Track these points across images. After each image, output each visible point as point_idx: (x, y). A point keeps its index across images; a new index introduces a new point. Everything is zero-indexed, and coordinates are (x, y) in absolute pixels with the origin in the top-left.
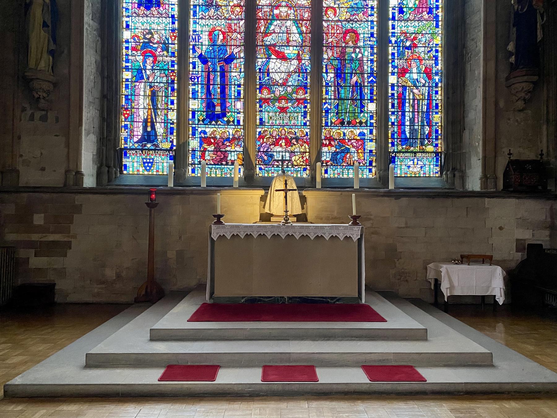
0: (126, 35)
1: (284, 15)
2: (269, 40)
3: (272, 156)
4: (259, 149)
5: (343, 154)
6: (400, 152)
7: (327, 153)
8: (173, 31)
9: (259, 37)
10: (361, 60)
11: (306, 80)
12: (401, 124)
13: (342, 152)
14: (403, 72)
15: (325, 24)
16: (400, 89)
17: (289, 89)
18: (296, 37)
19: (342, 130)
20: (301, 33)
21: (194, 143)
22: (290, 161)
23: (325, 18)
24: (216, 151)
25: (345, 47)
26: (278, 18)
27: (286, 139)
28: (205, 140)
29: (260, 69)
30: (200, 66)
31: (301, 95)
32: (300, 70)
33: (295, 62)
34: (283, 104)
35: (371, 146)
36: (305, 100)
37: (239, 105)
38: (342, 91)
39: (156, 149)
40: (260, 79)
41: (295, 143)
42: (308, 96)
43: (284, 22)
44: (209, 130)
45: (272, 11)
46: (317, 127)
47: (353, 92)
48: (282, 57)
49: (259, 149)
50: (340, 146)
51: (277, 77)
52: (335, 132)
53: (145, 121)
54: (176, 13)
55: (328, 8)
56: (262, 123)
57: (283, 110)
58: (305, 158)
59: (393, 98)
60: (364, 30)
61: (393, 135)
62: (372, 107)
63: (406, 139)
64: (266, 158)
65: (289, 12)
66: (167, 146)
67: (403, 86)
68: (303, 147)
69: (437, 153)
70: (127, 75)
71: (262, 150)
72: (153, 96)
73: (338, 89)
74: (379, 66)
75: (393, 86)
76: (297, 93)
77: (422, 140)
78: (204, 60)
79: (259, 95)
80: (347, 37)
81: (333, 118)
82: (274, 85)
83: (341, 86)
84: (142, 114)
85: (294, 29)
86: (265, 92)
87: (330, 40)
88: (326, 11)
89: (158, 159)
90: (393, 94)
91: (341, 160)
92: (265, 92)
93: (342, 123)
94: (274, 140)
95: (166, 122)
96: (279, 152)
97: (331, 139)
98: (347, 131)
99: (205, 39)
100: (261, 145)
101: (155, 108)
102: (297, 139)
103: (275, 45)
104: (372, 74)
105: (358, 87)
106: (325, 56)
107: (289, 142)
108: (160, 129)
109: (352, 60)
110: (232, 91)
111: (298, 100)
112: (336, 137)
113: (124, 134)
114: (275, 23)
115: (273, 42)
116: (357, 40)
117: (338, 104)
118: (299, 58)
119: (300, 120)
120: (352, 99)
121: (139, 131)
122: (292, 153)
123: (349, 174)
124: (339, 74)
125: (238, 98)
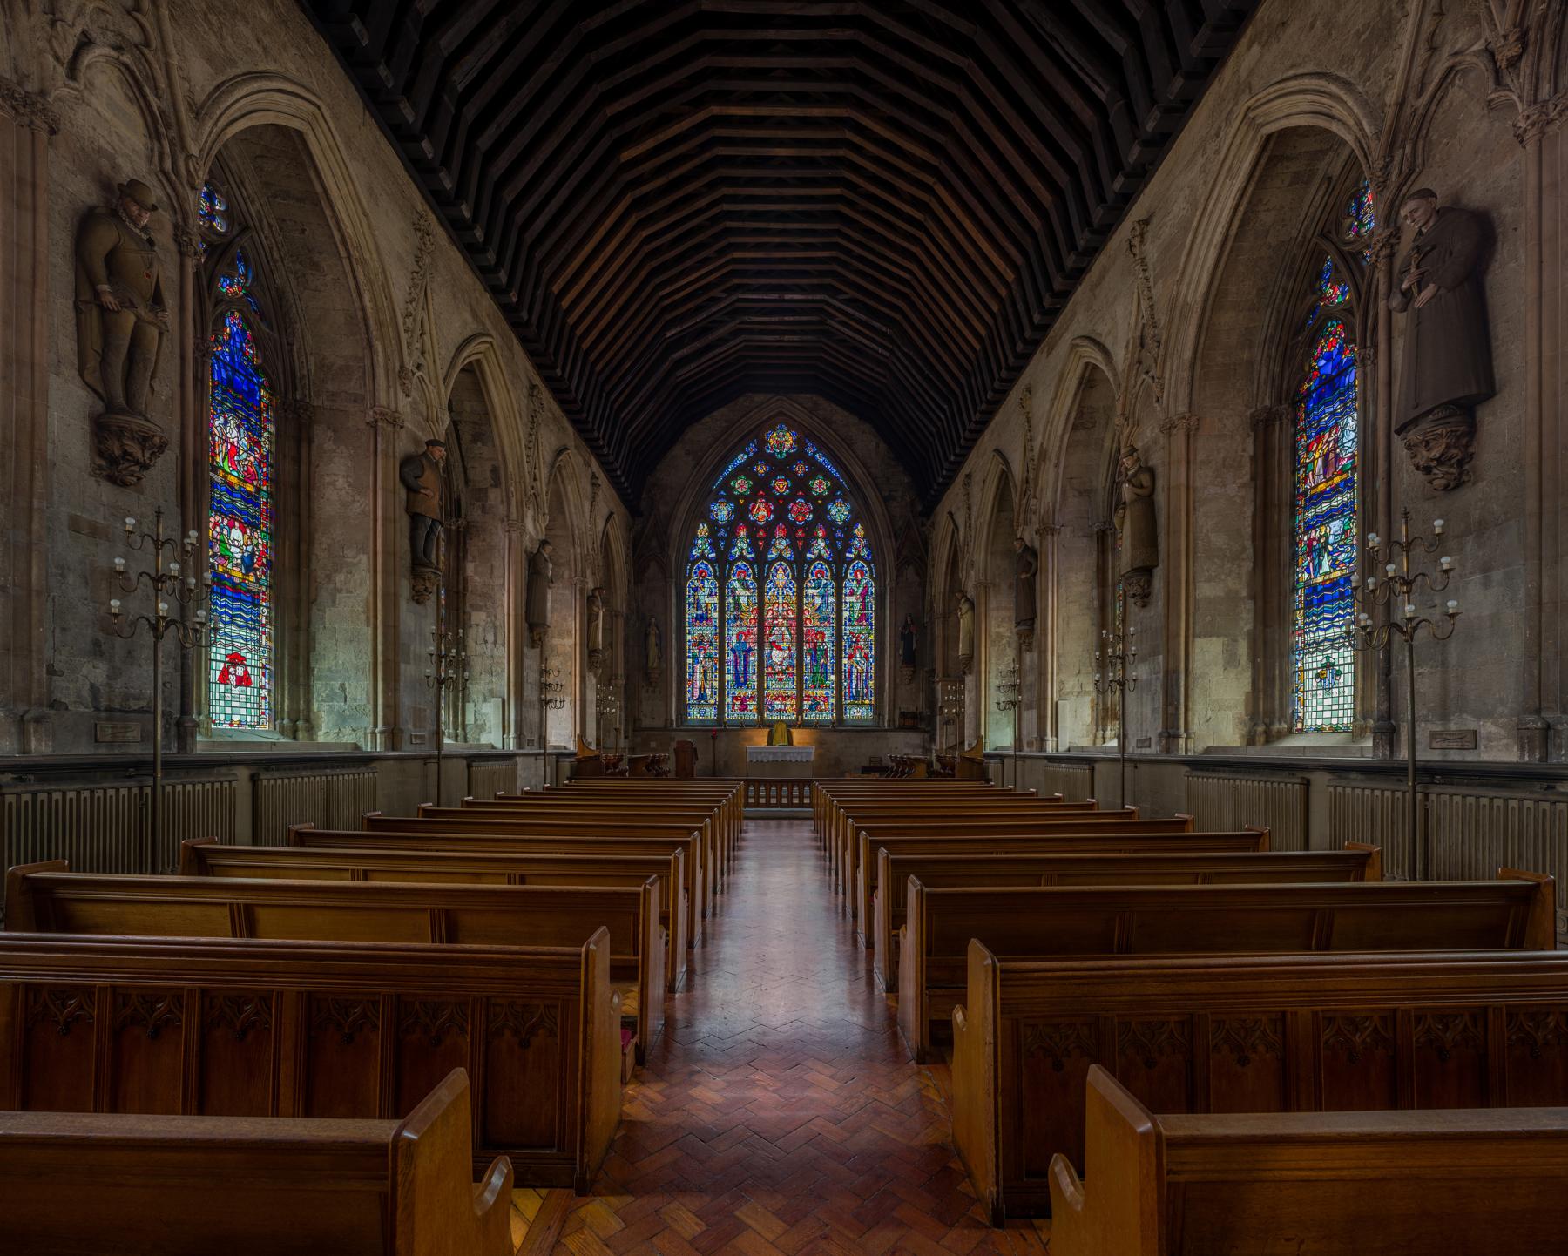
0: (689, 637)
2: (771, 638)
8: (716, 634)
10: (826, 650)
12: (850, 687)
14: (850, 657)
18: (787, 637)
19: (816, 691)
20: (790, 634)
21: (728, 700)
24: (741, 705)
26: (777, 625)
28: (735, 698)
30: (731, 656)
31: (791, 671)
32: (790, 656)
33: (787, 652)
34: (780, 676)
35: (832, 700)
37: (754, 677)
39: (707, 704)
42: (795, 671)
44: (737, 692)
46: (800, 689)
48: (780, 649)
51: (776, 660)
52: (810, 692)
53: (700, 688)
54: (717, 624)
56: (768, 688)
57: (780, 680)
60: (828, 633)
62: (833, 677)
66: (712, 701)
69: (871, 705)
70: (689, 661)
72: (705, 673)
74: (837, 653)
78: (734, 652)
81: (809, 684)
84: (698, 684)
89: (708, 710)
93: (815, 687)
95: (712, 688)
96: (778, 704)
97: (808, 696)
98: (818, 692)
99: (734, 639)
101: (706, 680)
104: (832, 658)
105: (825, 665)
107: (784, 699)
108: (709, 692)
110: (751, 669)
113: (688, 695)
116: (824, 638)
118: (789, 649)
119: (791, 686)
121: (697, 693)
122: (786, 705)
123: (821, 717)
124: (814, 658)
125: (754, 673)
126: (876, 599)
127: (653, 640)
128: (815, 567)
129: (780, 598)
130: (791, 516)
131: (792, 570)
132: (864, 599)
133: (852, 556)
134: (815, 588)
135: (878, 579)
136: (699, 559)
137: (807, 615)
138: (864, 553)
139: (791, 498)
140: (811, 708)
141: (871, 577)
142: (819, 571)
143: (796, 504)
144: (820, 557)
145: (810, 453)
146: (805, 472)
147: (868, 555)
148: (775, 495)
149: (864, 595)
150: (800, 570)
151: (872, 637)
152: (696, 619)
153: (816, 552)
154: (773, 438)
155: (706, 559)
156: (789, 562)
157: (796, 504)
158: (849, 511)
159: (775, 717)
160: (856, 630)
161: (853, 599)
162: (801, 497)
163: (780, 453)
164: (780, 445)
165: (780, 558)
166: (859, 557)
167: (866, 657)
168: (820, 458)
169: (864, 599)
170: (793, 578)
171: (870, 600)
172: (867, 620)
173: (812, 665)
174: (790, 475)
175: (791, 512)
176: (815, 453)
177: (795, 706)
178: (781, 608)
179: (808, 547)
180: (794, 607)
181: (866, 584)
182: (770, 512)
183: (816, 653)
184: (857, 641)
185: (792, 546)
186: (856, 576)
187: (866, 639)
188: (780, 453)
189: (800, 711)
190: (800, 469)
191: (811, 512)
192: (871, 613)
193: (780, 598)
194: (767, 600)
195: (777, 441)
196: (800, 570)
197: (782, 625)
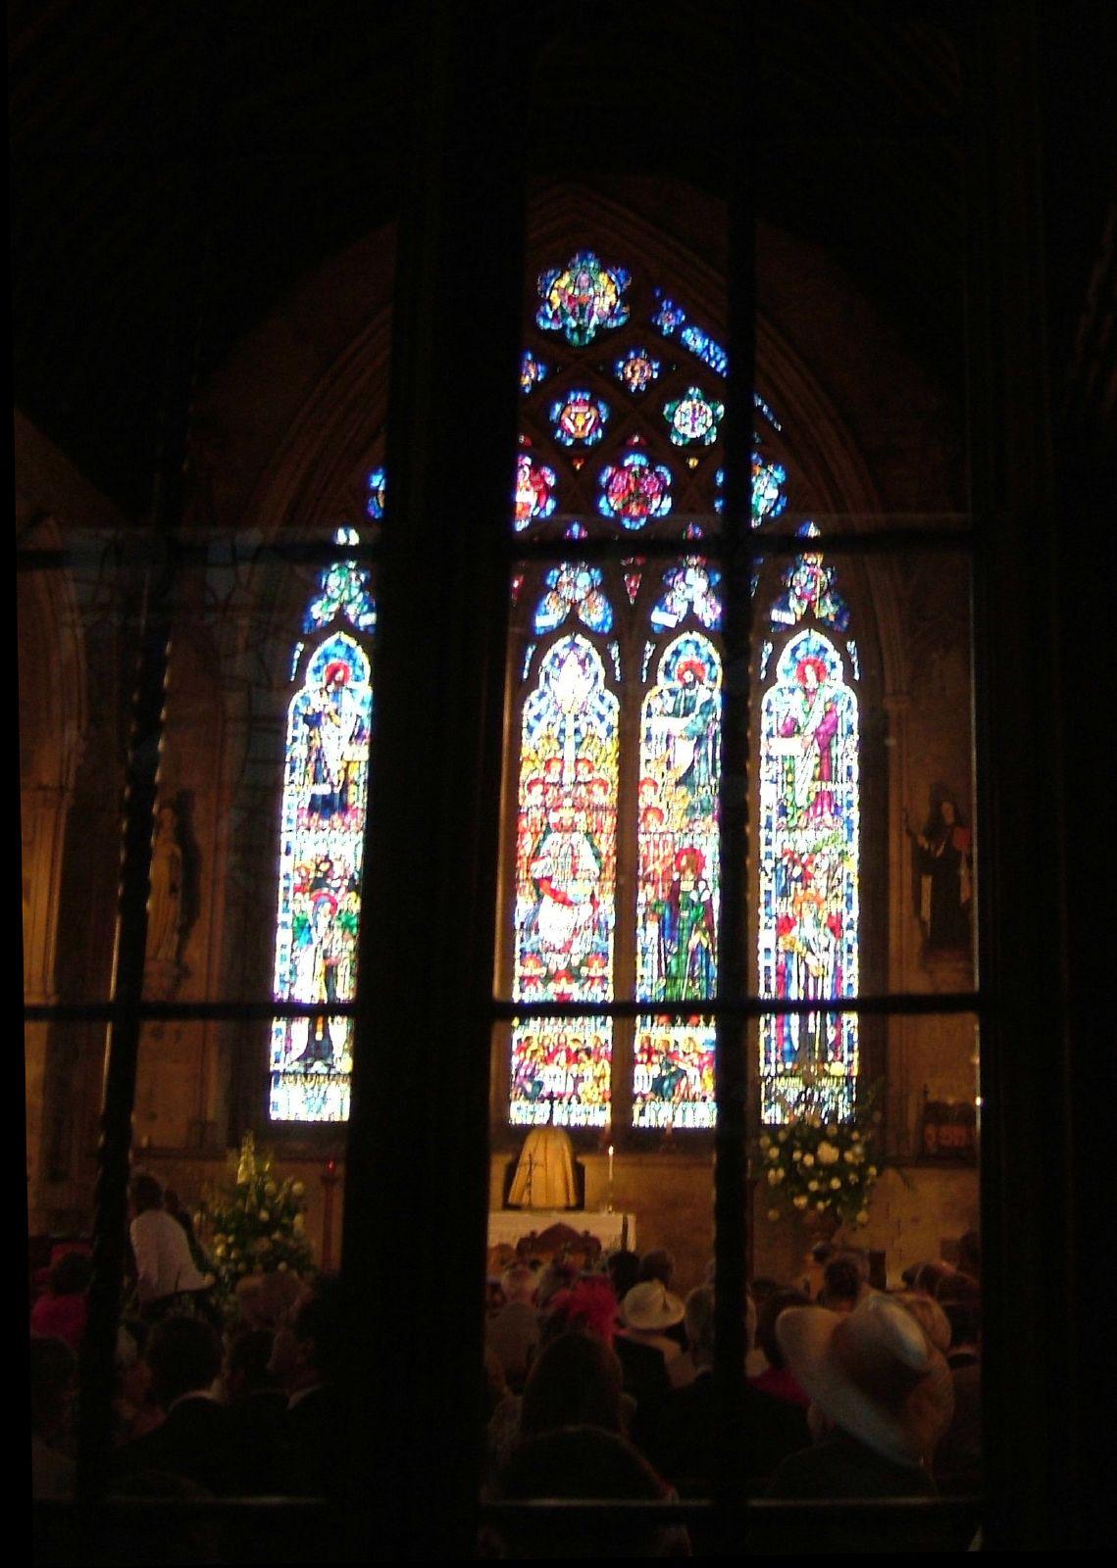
1: (567, 823)
2: (539, 869)
3: (540, 1084)
4: (517, 1071)
5: (673, 1081)
6: (779, 1075)
7: (644, 1076)
9: (522, 863)
11: (607, 940)
13: (673, 1075)
14: (785, 925)
15: (642, 839)
16: (782, 958)
17: (575, 962)
18: (588, 862)
20: (598, 856)
22: (575, 1093)
23: (642, 828)
25: (679, 881)
26: (560, 828)
27: (568, 1050)
29: (522, 924)
31: (596, 970)
32: (597, 926)
33: (586, 910)
36: (604, 978)
38: (673, 962)
40: (522, 941)
41: (585, 1058)
42: (609, 971)
43: (567, 836)
45: (546, 814)
47: (693, 964)
49: (517, 1071)
50: (669, 1066)
55: (648, 808)
58: (602, 1089)
59: (768, 976)
61: (768, 1040)
63: (792, 1050)
64: (529, 1087)
65: (576, 819)
67: (786, 952)
68: (600, 1066)
71: (522, 1073)
73: (666, 959)
75: (767, 950)
76: (589, 965)
77: (824, 1053)
79: (519, 970)
80: (684, 862)
82: (547, 951)
83: (668, 952)
85: (585, 850)
86: (531, 963)
87: (650, 869)
88: (645, 815)
90: (767, 968)
91: (670, 1092)
92: (531, 963)
94: (546, 1054)
97: (650, 1051)
100: (520, 1065)
102: (588, 1052)
103: (549, 879)
106: (641, 898)
109: (692, 905)
111: (588, 978)
112: (658, 1045)
114: (551, 838)
115: (546, 874)
117: (665, 988)
120: (692, 976)
122: (578, 1079)
126: (864, 747)
127: (158, 871)
128: (677, 653)
129: (570, 744)
130: (607, 506)
131: (608, 663)
132: (826, 748)
133: (788, 618)
134: (675, 714)
135: (869, 691)
136: (329, 629)
137: (647, 797)
138: (827, 610)
139: (610, 449)
140: (658, 1087)
141: (848, 678)
142: (689, 666)
143: (621, 468)
144: (691, 622)
145: (667, 328)
146: (650, 382)
147: (838, 617)
148: (560, 443)
149: (825, 738)
150: (633, 657)
151: (852, 866)
152: (312, 808)
153: (681, 608)
154: (559, 289)
155: (352, 630)
156: (600, 640)
157: (621, 468)
158: (781, 488)
159: (539, 1114)
160: (804, 841)
161: (792, 746)
162: (637, 449)
163: (581, 330)
164: (582, 309)
165: (572, 624)
166: (809, 620)
167: (835, 927)
168: (695, 340)
169: (826, 748)
170: (610, 683)
171: (847, 752)
172: (837, 811)
173: (663, 953)
174: (605, 387)
175: (606, 491)
176: (679, 329)
177: (606, 1084)
178: (569, 777)
179: (655, 592)
180: (610, 771)
181: (833, 701)
182: (546, 492)
183: (675, 915)
184: (805, 877)
185: (610, 589)
186: (803, 677)
187: (832, 870)
188: (581, 330)
189: (622, 1097)
190: (638, 373)
191: (664, 492)
192: (848, 791)
193: (570, 744)
194: (526, 750)
195: (571, 298)
196: (633, 657)
197: (573, 828)
